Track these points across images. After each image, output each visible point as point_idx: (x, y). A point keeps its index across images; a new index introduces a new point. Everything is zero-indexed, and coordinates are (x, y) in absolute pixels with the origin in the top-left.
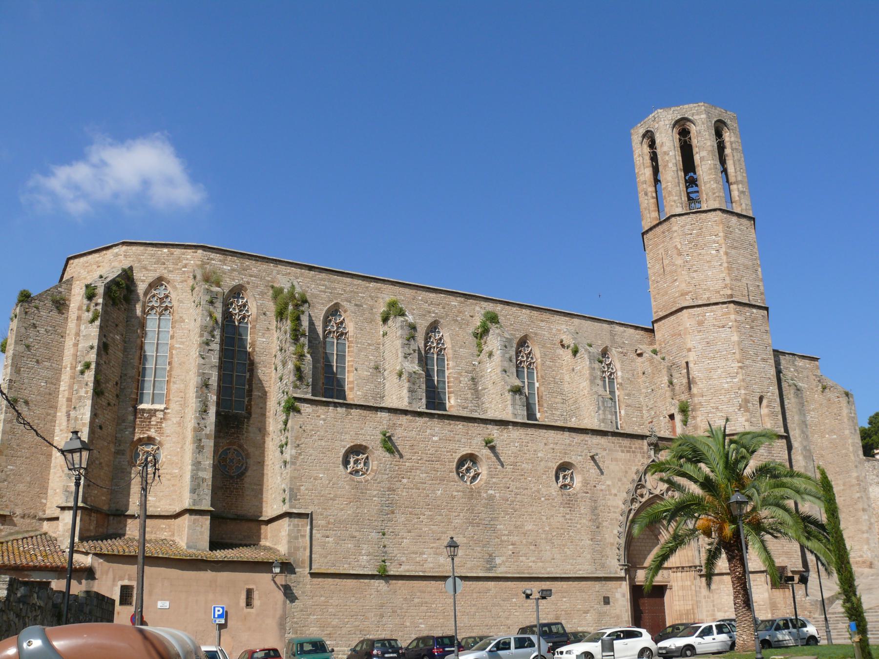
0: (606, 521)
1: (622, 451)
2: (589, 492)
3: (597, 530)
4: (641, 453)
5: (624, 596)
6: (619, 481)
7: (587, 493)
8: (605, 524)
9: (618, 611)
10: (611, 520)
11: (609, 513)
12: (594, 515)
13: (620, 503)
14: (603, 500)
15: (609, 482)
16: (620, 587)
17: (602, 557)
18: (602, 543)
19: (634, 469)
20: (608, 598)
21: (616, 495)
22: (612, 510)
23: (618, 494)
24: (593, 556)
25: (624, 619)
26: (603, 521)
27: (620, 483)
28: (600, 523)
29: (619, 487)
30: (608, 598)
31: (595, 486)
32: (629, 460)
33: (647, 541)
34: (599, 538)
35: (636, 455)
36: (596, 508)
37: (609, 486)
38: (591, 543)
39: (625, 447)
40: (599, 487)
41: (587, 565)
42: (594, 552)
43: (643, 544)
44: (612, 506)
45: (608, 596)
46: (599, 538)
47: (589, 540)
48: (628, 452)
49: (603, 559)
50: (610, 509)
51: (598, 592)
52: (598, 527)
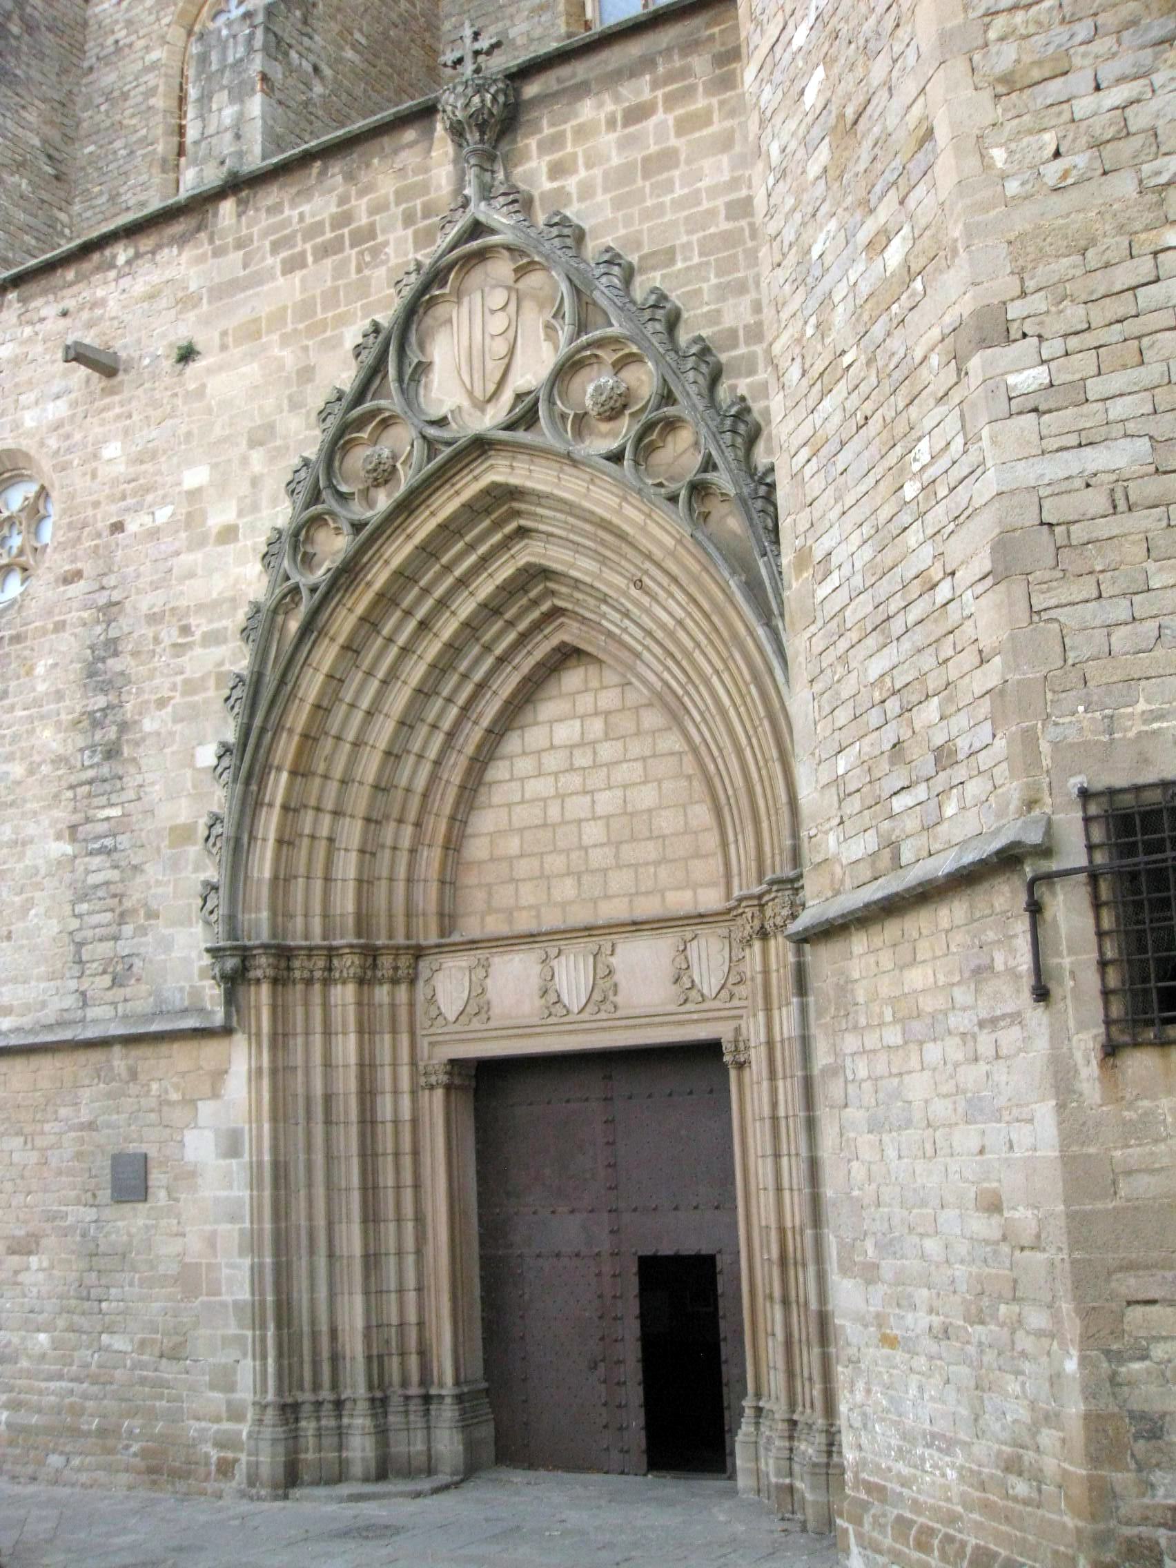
0: (162, 703)
1: (293, 265)
2: (87, 567)
3: (105, 770)
4: (409, 219)
5: (232, 1147)
6: (253, 443)
7: (78, 574)
8: (148, 725)
9: (194, 1244)
10: (191, 687)
11: (179, 649)
12: (103, 688)
13: (254, 568)
14: (155, 586)
15: (197, 476)
16: (215, 1095)
17: (122, 918)
18: (124, 840)
19: (352, 335)
20: (120, 1162)
21: (229, 534)
22: (201, 625)
23: (241, 522)
24: (74, 924)
25: (227, 1298)
26: (142, 710)
27: (257, 459)
28: (124, 727)
29: (255, 482)
30: (120, 1162)
31: (118, 527)
32: (331, 298)
33: (607, 751)
34: (115, 812)
35: (375, 252)
36: (112, 647)
37: (194, 495)
38: (69, 849)
39: (315, 230)
40: (132, 527)
41: (39, 979)
42: (83, 897)
43: (574, 781)
44: (200, 608)
45: (144, 1148)
46: (115, 812)
47: (59, 837)
48: (324, 251)
49: (128, 930)
50: (185, 630)
51: (91, 1126)
52: (112, 753)
